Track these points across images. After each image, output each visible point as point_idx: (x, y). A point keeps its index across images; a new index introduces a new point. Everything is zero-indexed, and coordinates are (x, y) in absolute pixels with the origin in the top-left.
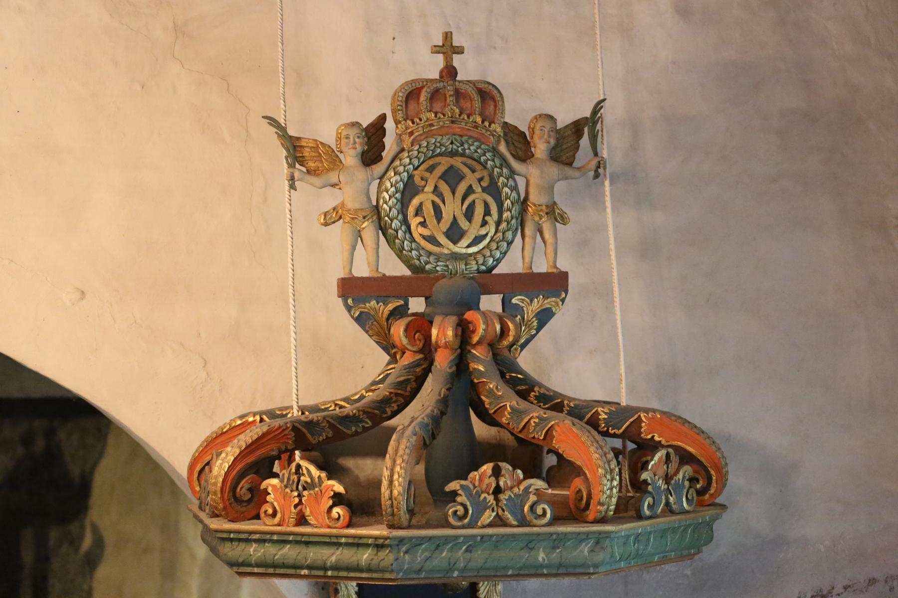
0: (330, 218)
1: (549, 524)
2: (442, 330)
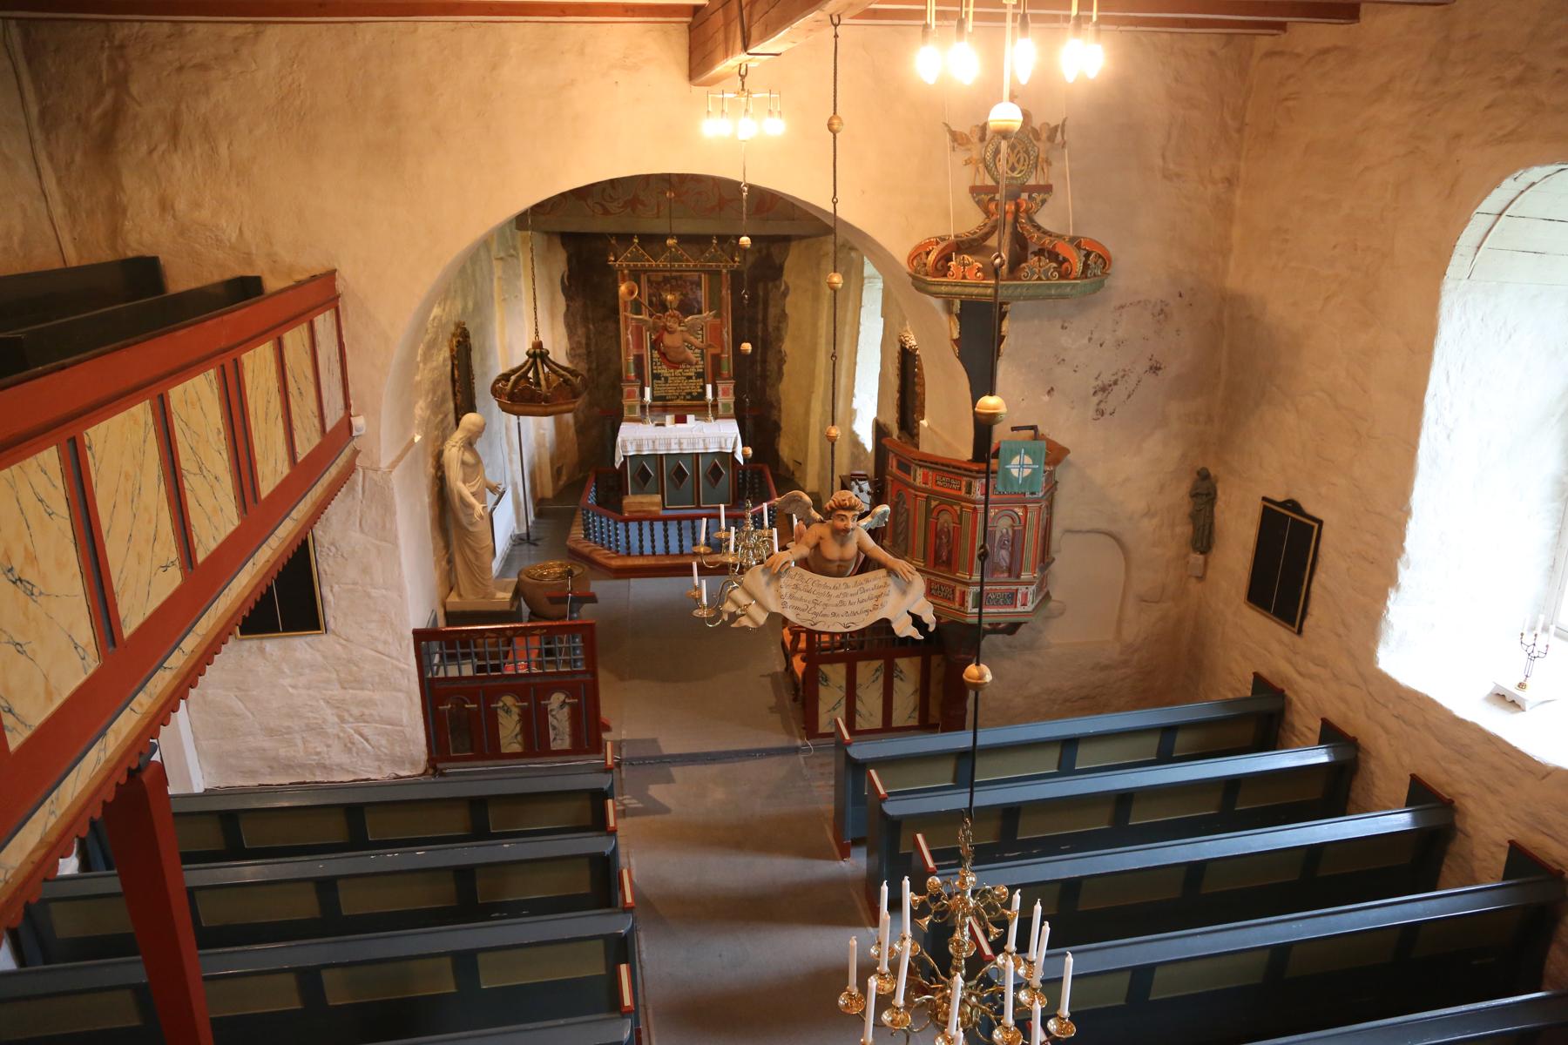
0: (967, 163)
1: (1057, 280)
2: (1010, 206)
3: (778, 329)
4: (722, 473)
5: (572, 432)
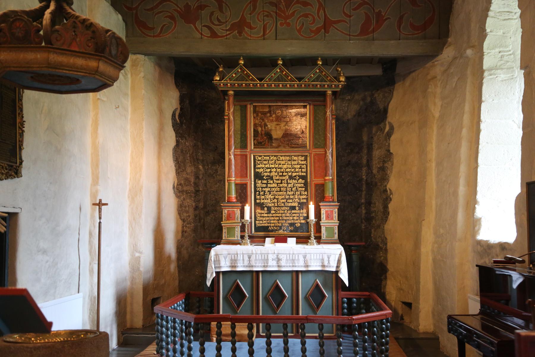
3: (383, 169)
4: (324, 296)
5: (173, 267)
